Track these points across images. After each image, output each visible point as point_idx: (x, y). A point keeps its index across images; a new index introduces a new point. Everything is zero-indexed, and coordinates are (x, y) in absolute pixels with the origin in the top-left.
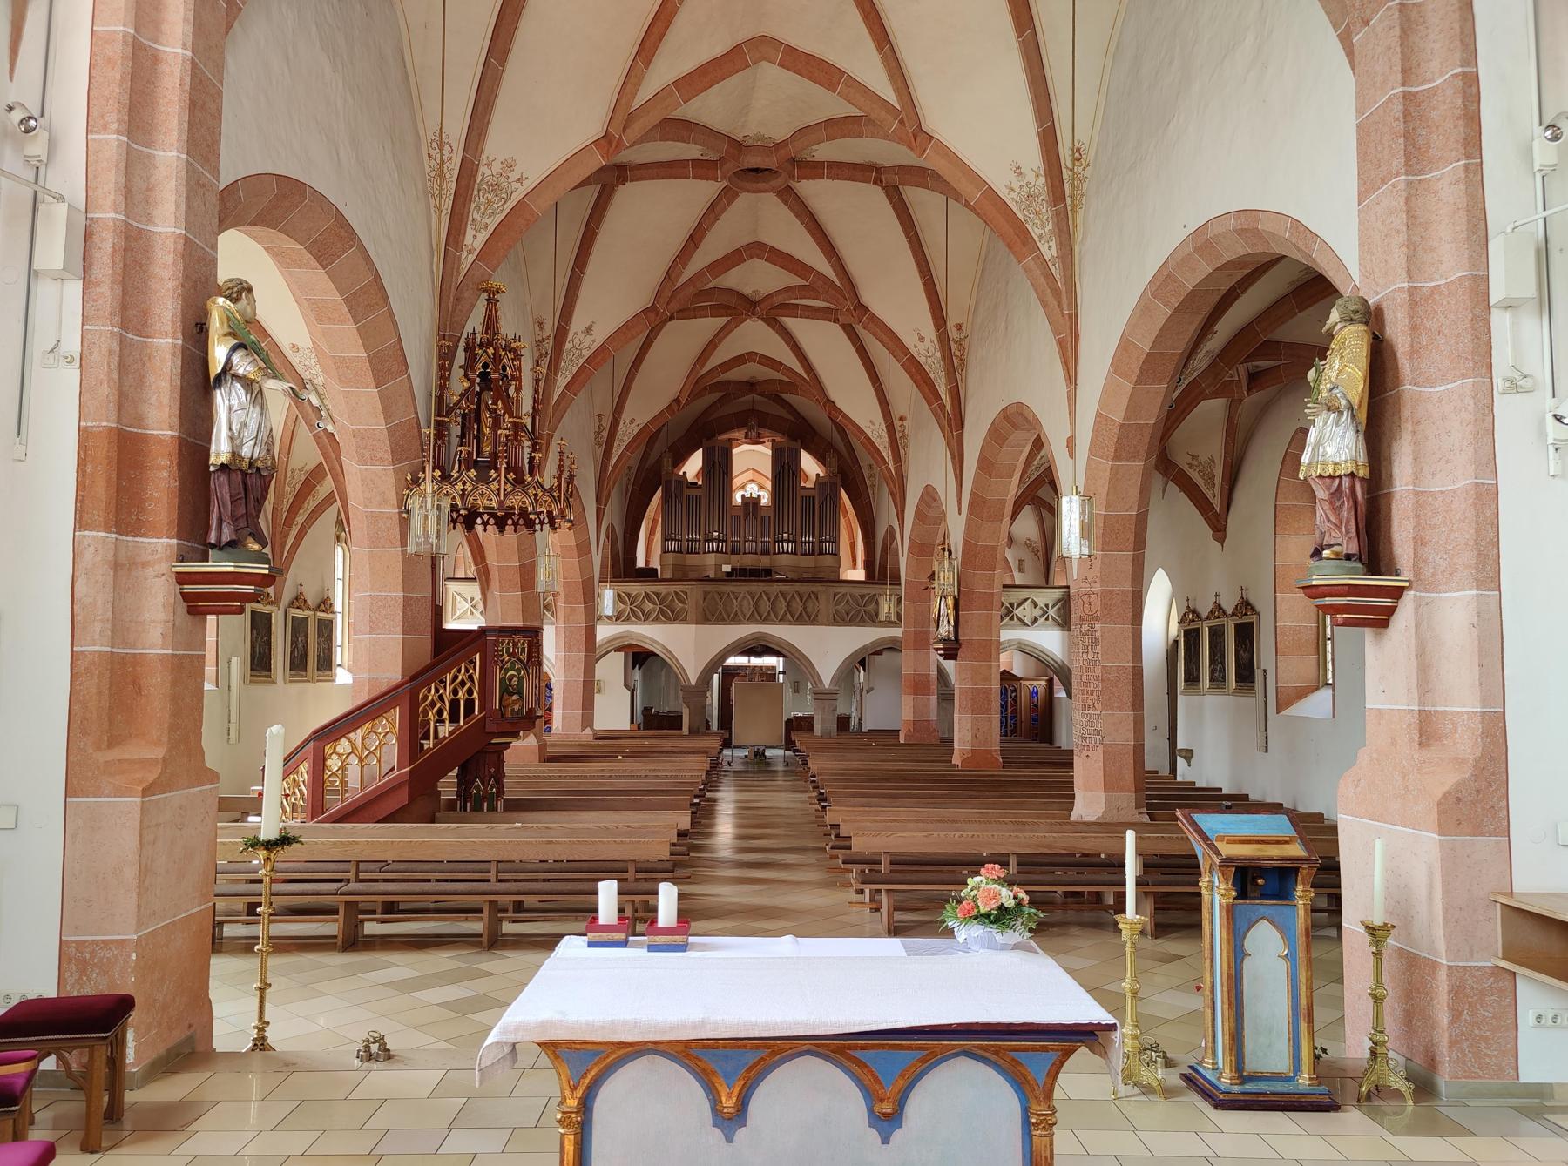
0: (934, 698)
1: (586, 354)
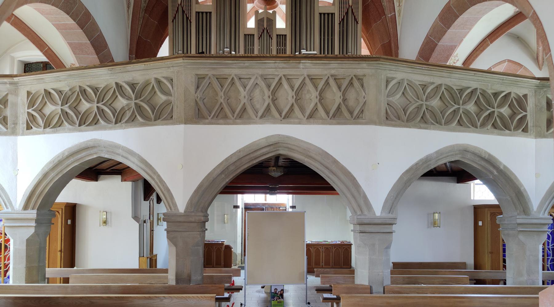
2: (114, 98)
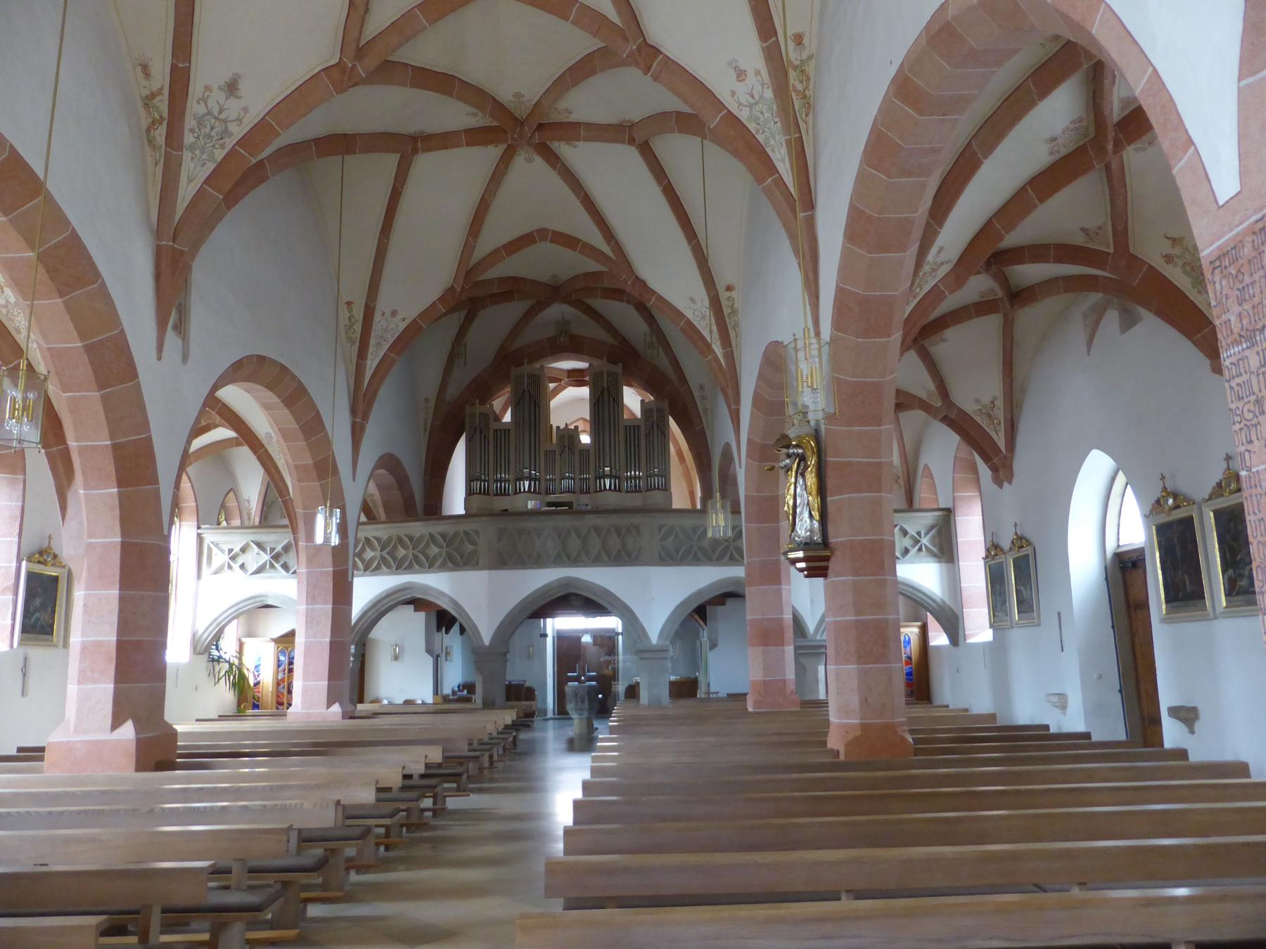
0: (789, 650)
1: (238, 131)
2: (428, 545)
